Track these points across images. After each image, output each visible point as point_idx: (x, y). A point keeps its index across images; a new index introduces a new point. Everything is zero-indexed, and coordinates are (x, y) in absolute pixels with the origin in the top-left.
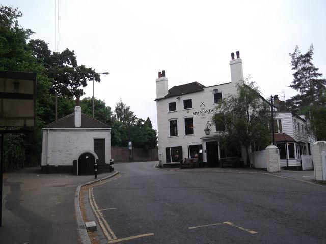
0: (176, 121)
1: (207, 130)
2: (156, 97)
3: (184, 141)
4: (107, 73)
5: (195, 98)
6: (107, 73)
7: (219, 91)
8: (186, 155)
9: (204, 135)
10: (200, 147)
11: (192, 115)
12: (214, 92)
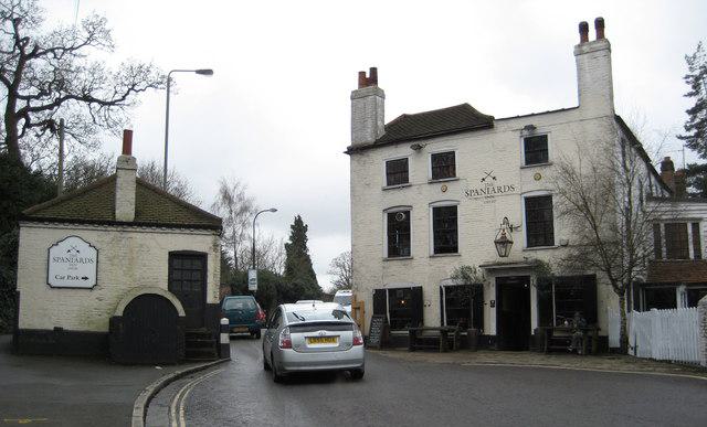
0: (408, 213)
1: (503, 243)
3: (427, 272)
4: (208, 72)
5: (465, 148)
6: (208, 72)
7: (540, 131)
8: (433, 316)
9: (490, 255)
10: (478, 291)
12: (526, 133)
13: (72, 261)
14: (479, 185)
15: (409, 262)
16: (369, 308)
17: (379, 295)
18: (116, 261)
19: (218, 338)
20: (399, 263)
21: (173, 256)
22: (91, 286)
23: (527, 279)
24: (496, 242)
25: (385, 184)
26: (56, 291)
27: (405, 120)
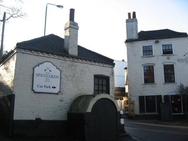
0: (153, 67)
2: (125, 38)
4: (59, 6)
5: (174, 43)
6: (59, 6)
13: (48, 76)
14: (183, 58)
15: (154, 85)
16: (137, 104)
17: (141, 98)
18: (70, 78)
19: (120, 121)
20: (149, 86)
21: (96, 77)
22: (56, 92)
25: (142, 55)
26: (37, 95)
27: (142, 32)
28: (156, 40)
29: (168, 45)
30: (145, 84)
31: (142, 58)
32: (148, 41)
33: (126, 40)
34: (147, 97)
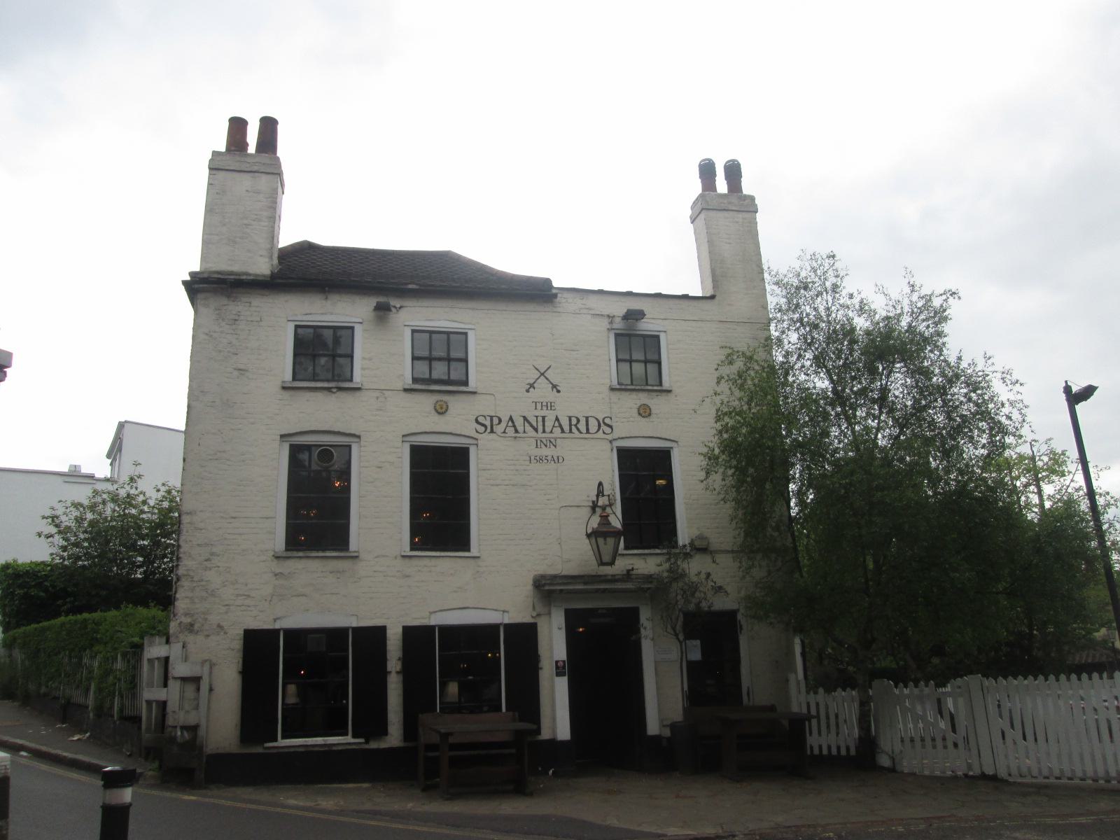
2: (194, 264)
7: (646, 326)
11: (470, 429)
12: (619, 324)
23: (629, 620)
24: (589, 536)
25: (288, 376)
27: (306, 250)
28: (382, 299)
29: (448, 333)
30: (289, 554)
31: (287, 394)
32: (334, 298)
33: (192, 274)
34: (296, 637)
